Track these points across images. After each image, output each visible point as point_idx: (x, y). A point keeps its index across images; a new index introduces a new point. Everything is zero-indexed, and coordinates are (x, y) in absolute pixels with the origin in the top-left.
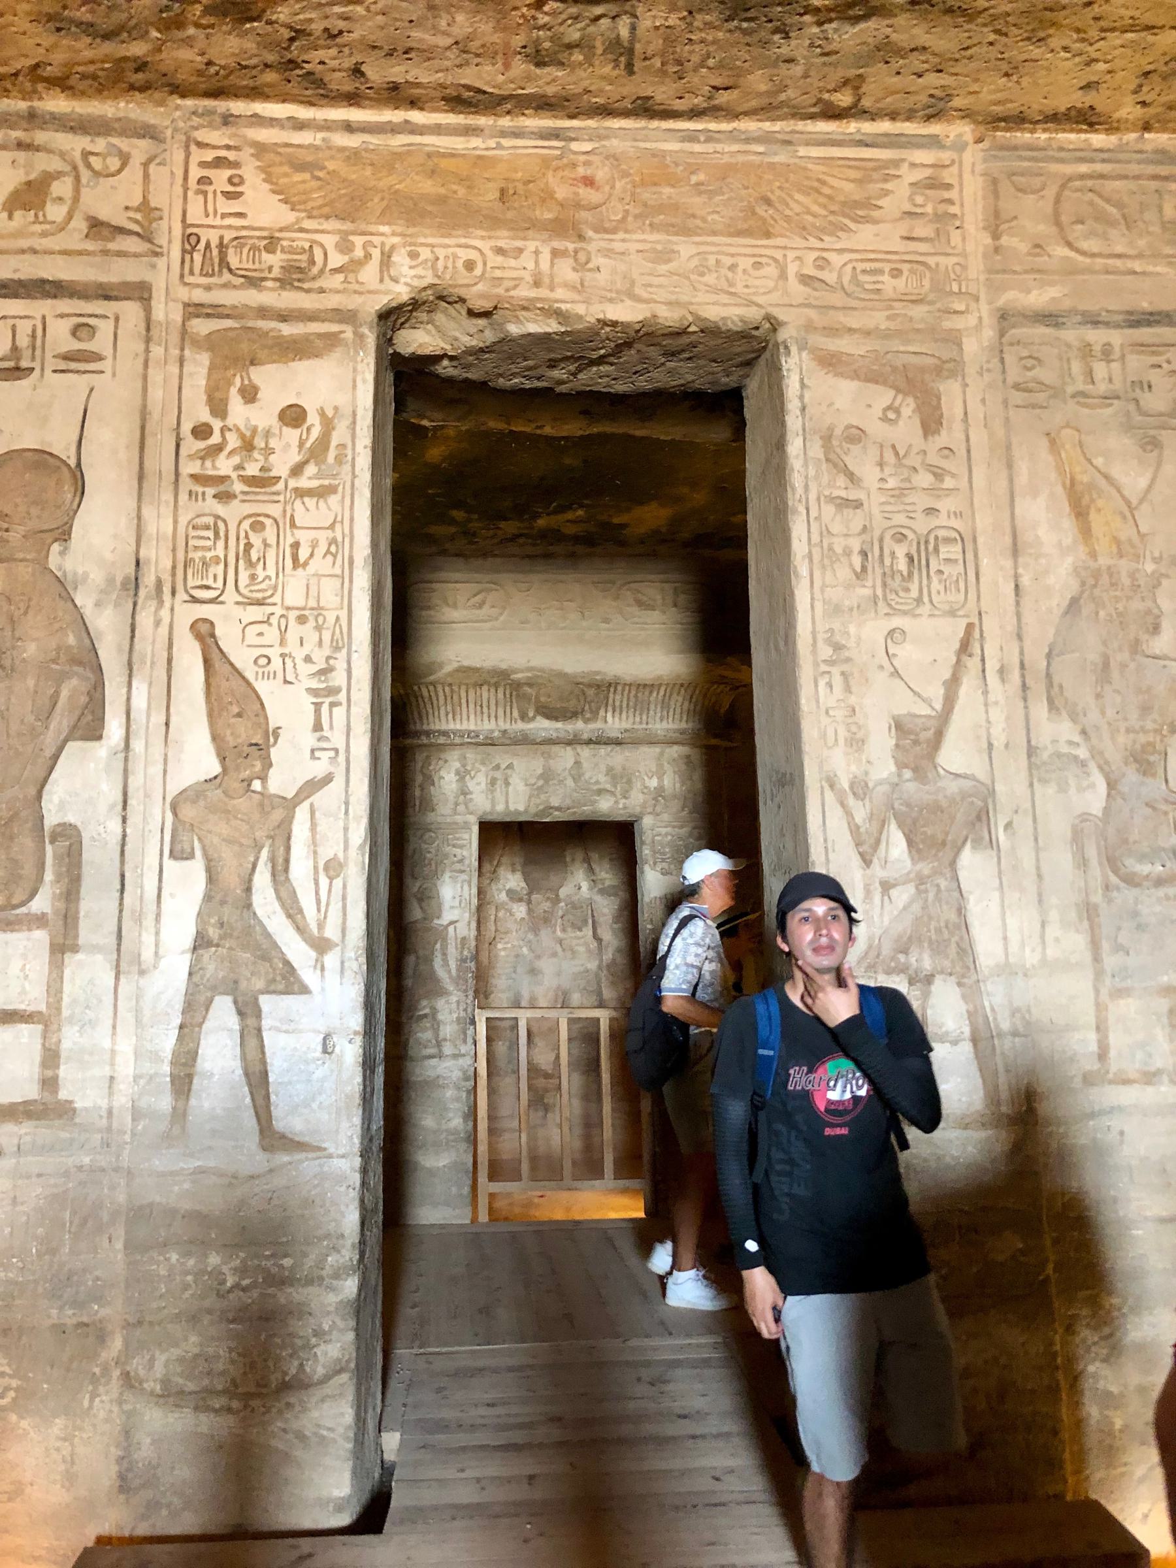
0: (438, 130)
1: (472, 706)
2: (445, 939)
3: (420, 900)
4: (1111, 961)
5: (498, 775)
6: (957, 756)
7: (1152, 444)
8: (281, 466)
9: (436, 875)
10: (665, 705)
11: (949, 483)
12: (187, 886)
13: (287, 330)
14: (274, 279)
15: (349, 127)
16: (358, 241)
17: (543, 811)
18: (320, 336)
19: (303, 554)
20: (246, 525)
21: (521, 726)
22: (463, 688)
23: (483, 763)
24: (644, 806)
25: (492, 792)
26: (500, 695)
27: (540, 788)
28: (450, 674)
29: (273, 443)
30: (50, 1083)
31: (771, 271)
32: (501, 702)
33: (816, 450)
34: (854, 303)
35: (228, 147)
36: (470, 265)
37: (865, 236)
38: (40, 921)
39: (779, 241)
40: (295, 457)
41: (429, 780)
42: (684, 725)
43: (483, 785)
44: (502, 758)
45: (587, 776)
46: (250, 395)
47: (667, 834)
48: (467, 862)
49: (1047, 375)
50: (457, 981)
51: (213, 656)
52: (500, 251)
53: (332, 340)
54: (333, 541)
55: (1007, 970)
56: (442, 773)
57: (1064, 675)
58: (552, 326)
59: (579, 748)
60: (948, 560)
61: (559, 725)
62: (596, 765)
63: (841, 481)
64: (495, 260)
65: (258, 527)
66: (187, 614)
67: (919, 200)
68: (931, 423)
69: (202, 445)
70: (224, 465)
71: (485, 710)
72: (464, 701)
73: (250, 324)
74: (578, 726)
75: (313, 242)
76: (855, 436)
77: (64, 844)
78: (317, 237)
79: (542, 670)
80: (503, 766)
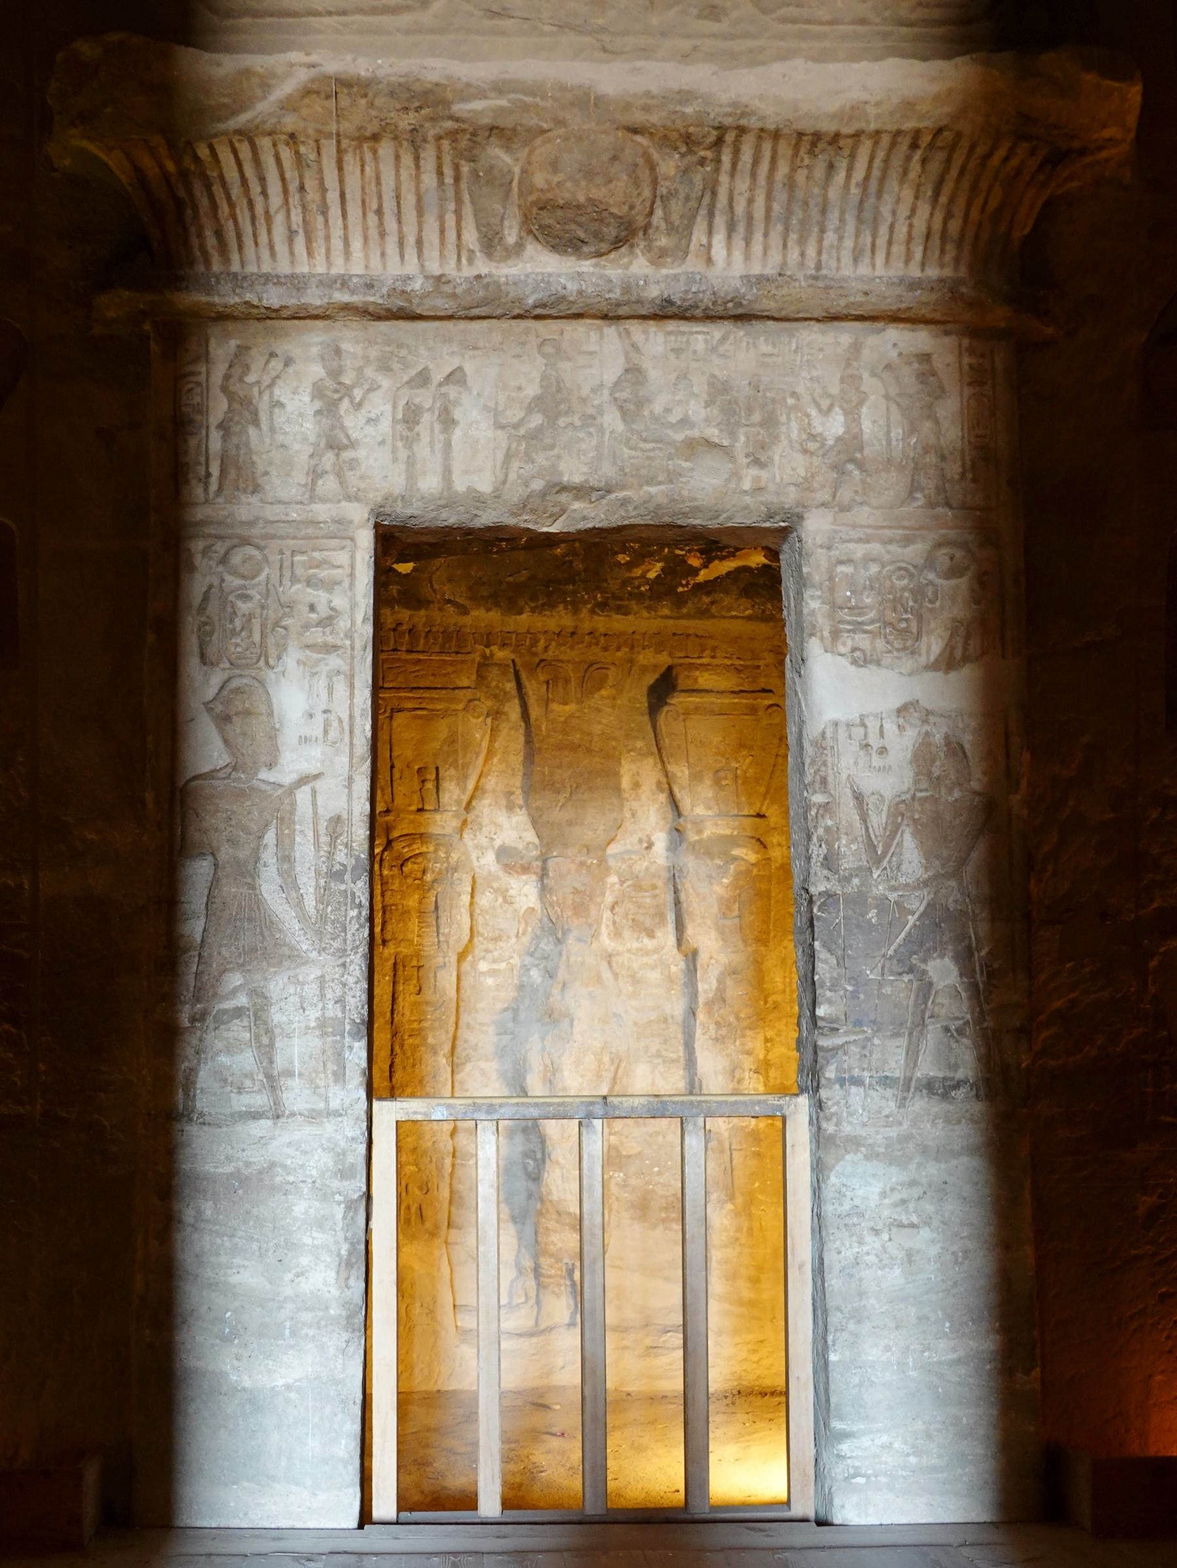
1: (354, 211)
2: (286, 820)
3: (224, 720)
5: (424, 398)
9: (263, 656)
10: (867, 219)
17: (543, 494)
21: (483, 266)
22: (329, 149)
23: (385, 367)
24: (805, 486)
25: (409, 442)
26: (429, 179)
27: (533, 436)
28: (288, 105)
32: (431, 199)
41: (244, 409)
42: (915, 272)
43: (385, 426)
44: (434, 350)
45: (657, 408)
47: (868, 559)
48: (343, 624)
50: (318, 927)
56: (281, 392)
59: (635, 327)
61: (586, 266)
62: (683, 376)
71: (391, 224)
72: (333, 197)
74: (638, 271)
79: (534, 90)
80: (438, 377)
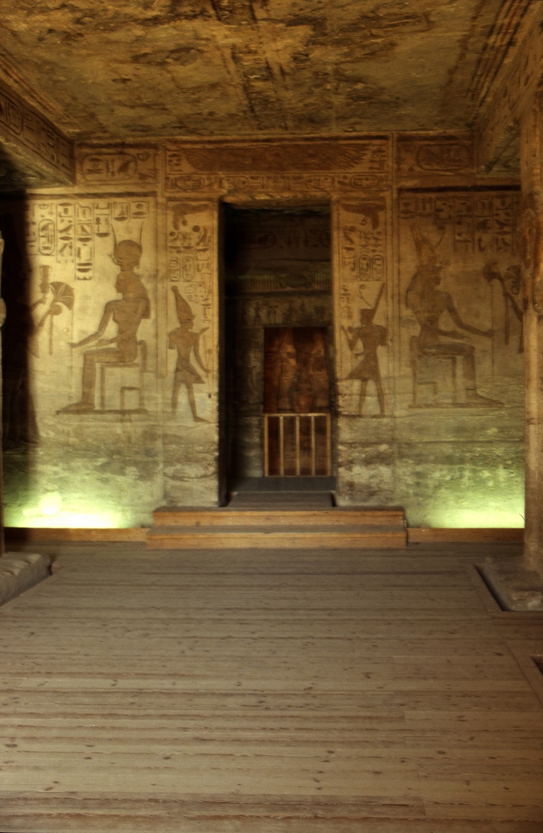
0: (235, 141)
4: (419, 376)
6: (378, 320)
7: (442, 228)
8: (193, 243)
11: (380, 242)
12: (173, 356)
13: (194, 204)
14: (191, 189)
15: (210, 142)
16: (212, 176)
18: (203, 205)
19: (200, 268)
20: (185, 261)
29: (192, 237)
30: (141, 404)
31: (330, 180)
33: (342, 234)
34: (353, 189)
35: (176, 151)
36: (244, 183)
37: (359, 169)
38: (137, 365)
39: (333, 171)
40: (197, 240)
46: (185, 223)
49: (412, 208)
51: (178, 297)
52: (252, 178)
53: (206, 206)
54: (208, 264)
55: (388, 378)
57: (411, 296)
58: (268, 198)
60: (379, 265)
63: (348, 242)
64: (251, 180)
65: (188, 260)
66: (170, 284)
67: (375, 156)
68: (375, 224)
69: (172, 238)
70: (178, 243)
73: (184, 203)
75: (201, 178)
76: (352, 229)
77: (142, 346)
78: (202, 176)
